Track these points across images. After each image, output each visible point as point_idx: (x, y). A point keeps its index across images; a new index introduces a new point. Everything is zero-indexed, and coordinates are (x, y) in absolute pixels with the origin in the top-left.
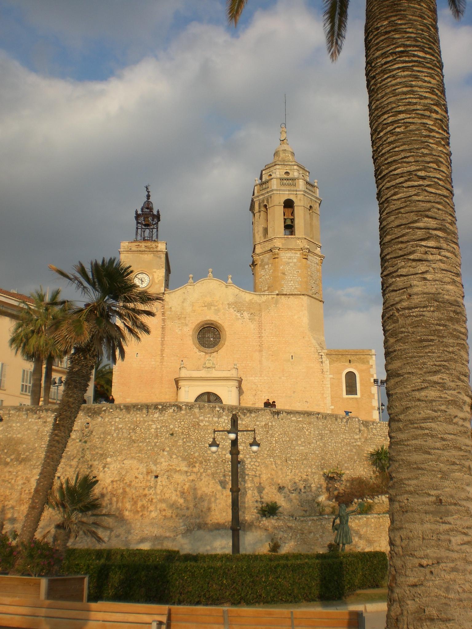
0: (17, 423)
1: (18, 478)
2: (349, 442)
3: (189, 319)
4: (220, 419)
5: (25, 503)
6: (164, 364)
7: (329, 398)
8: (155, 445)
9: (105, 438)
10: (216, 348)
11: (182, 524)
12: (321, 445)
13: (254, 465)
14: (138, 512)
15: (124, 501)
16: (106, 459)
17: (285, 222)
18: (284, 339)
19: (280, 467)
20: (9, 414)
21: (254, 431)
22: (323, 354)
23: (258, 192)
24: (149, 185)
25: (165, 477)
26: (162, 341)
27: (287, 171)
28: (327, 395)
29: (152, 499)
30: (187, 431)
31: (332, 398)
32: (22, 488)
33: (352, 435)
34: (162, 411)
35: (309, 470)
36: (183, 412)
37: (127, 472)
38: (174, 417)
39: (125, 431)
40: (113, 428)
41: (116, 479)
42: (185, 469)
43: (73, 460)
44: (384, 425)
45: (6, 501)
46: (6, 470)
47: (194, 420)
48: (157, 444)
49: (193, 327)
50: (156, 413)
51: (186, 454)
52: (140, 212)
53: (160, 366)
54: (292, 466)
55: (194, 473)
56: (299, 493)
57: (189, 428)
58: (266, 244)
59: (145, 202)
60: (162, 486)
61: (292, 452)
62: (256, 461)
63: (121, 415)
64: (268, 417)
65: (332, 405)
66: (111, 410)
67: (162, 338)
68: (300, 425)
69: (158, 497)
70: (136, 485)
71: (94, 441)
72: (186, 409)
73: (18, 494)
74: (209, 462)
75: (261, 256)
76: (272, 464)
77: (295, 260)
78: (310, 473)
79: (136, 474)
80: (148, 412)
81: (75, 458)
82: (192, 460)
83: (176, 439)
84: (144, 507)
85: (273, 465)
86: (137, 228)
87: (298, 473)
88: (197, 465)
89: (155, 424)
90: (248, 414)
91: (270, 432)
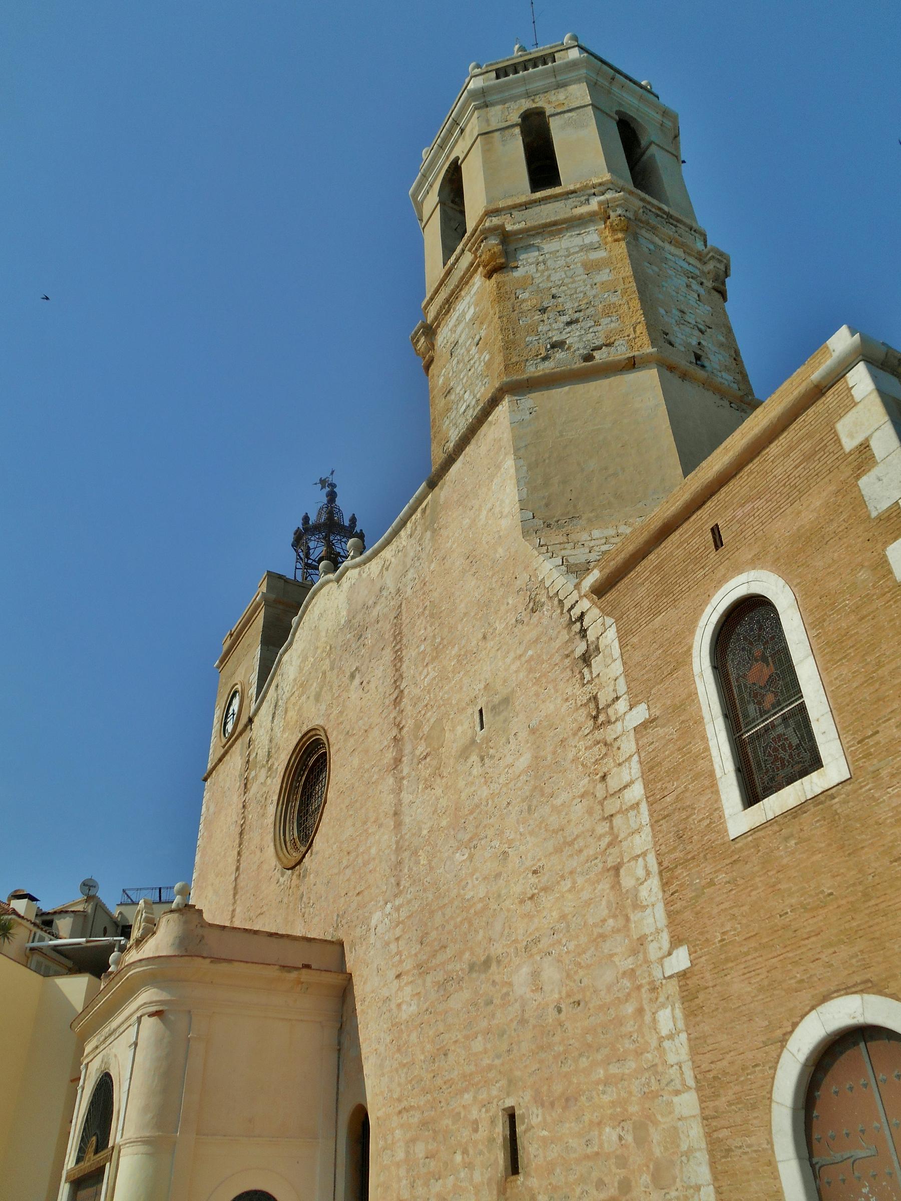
65: (676, 942)
67: (238, 869)
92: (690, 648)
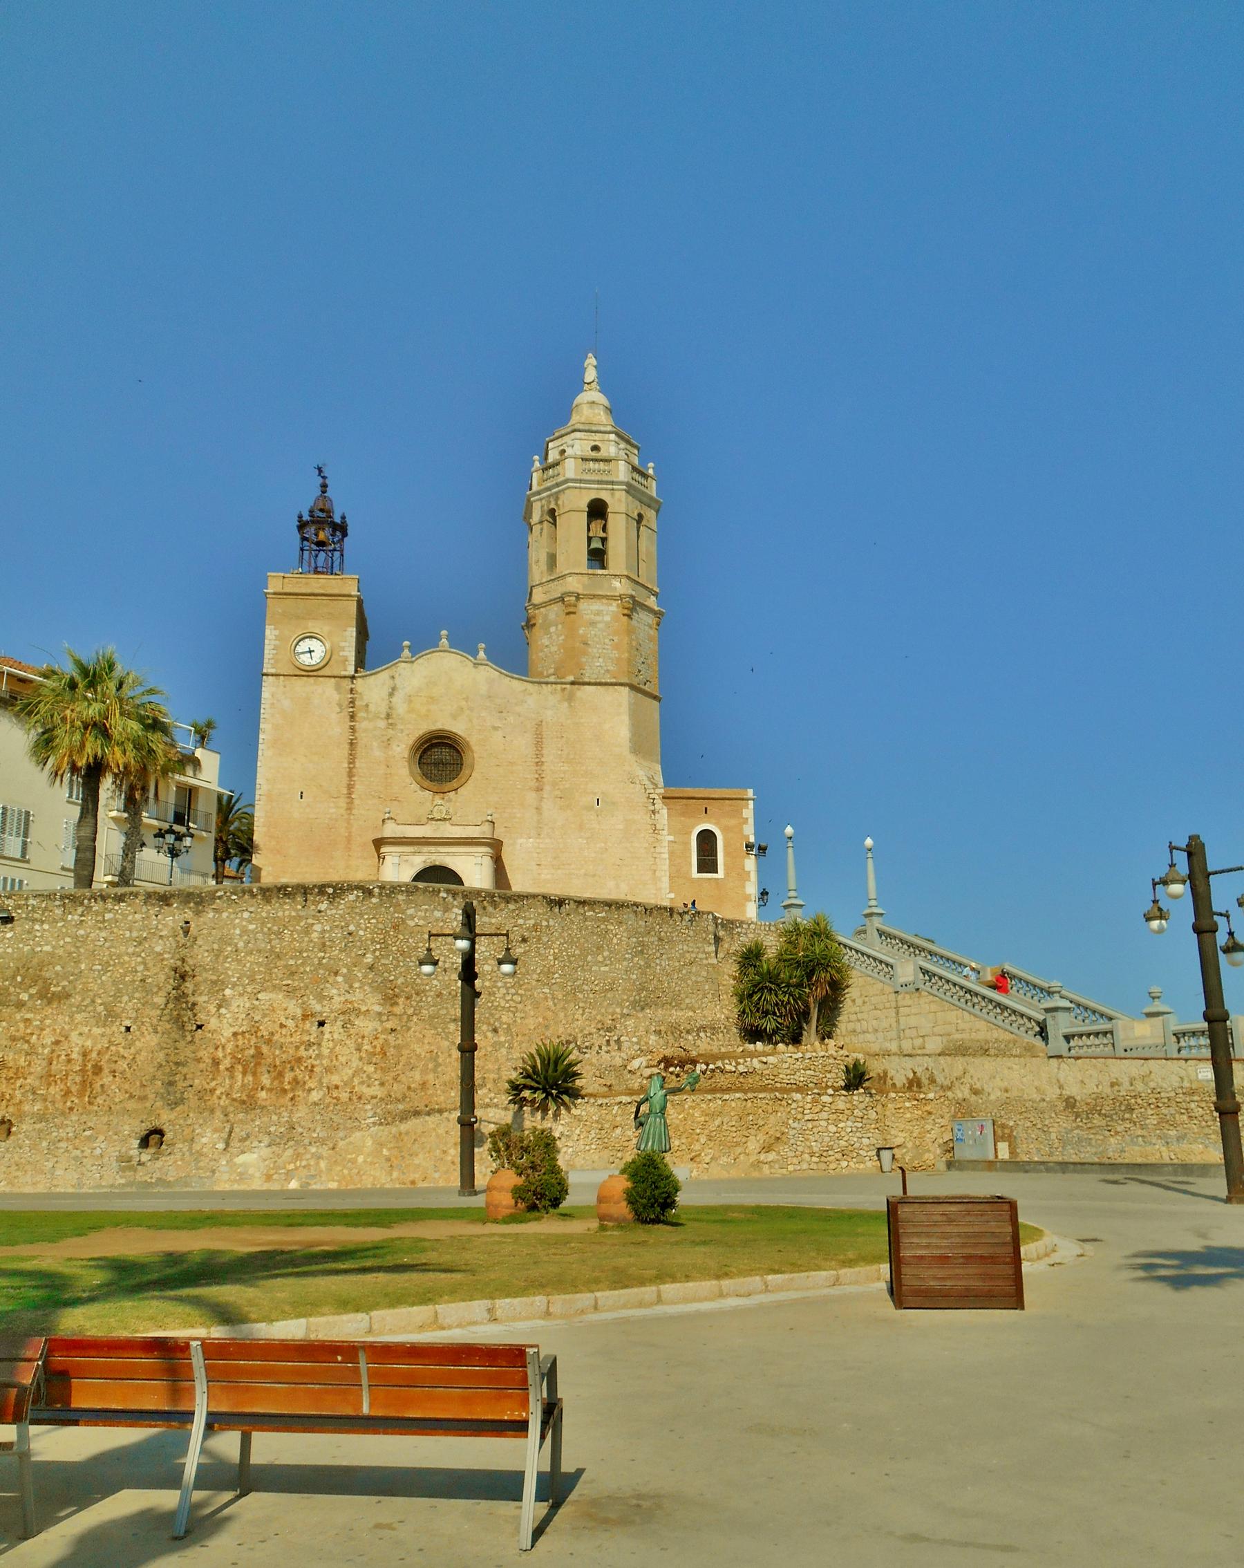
0: (42, 922)
1: (44, 1032)
2: (695, 958)
3: (402, 727)
4: (446, 914)
5: (59, 1082)
6: (353, 812)
7: (666, 880)
8: (320, 963)
9: (220, 951)
10: (455, 784)
11: (370, 1114)
12: (642, 963)
13: (512, 1000)
14: (285, 1091)
15: (259, 1070)
16: (223, 990)
17: (589, 545)
18: (584, 768)
19: (562, 1005)
20: (28, 906)
21: (507, 935)
22: (656, 797)
23: (539, 484)
24: (325, 465)
25: (339, 1023)
26: (349, 768)
27: (597, 443)
28: (663, 873)
29: (313, 1066)
30: (382, 936)
31: (671, 878)
32: (53, 1051)
33: (700, 945)
34: (334, 898)
35: (618, 1010)
36: (374, 900)
37: (264, 1016)
38: (357, 910)
39: (260, 936)
40: (238, 932)
41: (244, 1029)
42: (378, 1008)
43: (157, 993)
44: (763, 928)
45: (19, 1078)
46: (18, 1016)
47: (396, 915)
48: (324, 961)
49: (411, 742)
50: (323, 903)
51: (379, 981)
52: (306, 517)
53: (346, 817)
54: (585, 1002)
55: (396, 1015)
56: (598, 1053)
57: (386, 931)
58: (552, 585)
59: (317, 499)
60: (332, 1041)
61: (585, 977)
62: (517, 994)
63: (252, 906)
64: (540, 911)
66: (234, 897)
67: (350, 763)
68: (602, 926)
69: (324, 1062)
70: (282, 1040)
71: (200, 957)
72: (380, 894)
73: (44, 1063)
74: (425, 995)
75: (542, 609)
76: (546, 998)
77: (607, 618)
78: (619, 1016)
79: (283, 1020)
80: (306, 901)
81: (160, 989)
82: (391, 992)
83: (360, 953)
84: (298, 1083)
85: (549, 1000)
86: (302, 550)
87: (597, 1015)
88: (401, 1001)
89: (320, 923)
90: (503, 905)
91: (545, 939)
92: (691, 832)
